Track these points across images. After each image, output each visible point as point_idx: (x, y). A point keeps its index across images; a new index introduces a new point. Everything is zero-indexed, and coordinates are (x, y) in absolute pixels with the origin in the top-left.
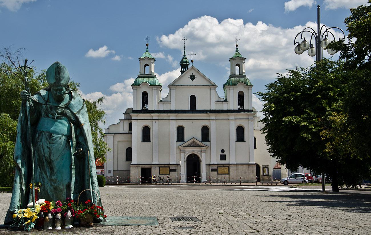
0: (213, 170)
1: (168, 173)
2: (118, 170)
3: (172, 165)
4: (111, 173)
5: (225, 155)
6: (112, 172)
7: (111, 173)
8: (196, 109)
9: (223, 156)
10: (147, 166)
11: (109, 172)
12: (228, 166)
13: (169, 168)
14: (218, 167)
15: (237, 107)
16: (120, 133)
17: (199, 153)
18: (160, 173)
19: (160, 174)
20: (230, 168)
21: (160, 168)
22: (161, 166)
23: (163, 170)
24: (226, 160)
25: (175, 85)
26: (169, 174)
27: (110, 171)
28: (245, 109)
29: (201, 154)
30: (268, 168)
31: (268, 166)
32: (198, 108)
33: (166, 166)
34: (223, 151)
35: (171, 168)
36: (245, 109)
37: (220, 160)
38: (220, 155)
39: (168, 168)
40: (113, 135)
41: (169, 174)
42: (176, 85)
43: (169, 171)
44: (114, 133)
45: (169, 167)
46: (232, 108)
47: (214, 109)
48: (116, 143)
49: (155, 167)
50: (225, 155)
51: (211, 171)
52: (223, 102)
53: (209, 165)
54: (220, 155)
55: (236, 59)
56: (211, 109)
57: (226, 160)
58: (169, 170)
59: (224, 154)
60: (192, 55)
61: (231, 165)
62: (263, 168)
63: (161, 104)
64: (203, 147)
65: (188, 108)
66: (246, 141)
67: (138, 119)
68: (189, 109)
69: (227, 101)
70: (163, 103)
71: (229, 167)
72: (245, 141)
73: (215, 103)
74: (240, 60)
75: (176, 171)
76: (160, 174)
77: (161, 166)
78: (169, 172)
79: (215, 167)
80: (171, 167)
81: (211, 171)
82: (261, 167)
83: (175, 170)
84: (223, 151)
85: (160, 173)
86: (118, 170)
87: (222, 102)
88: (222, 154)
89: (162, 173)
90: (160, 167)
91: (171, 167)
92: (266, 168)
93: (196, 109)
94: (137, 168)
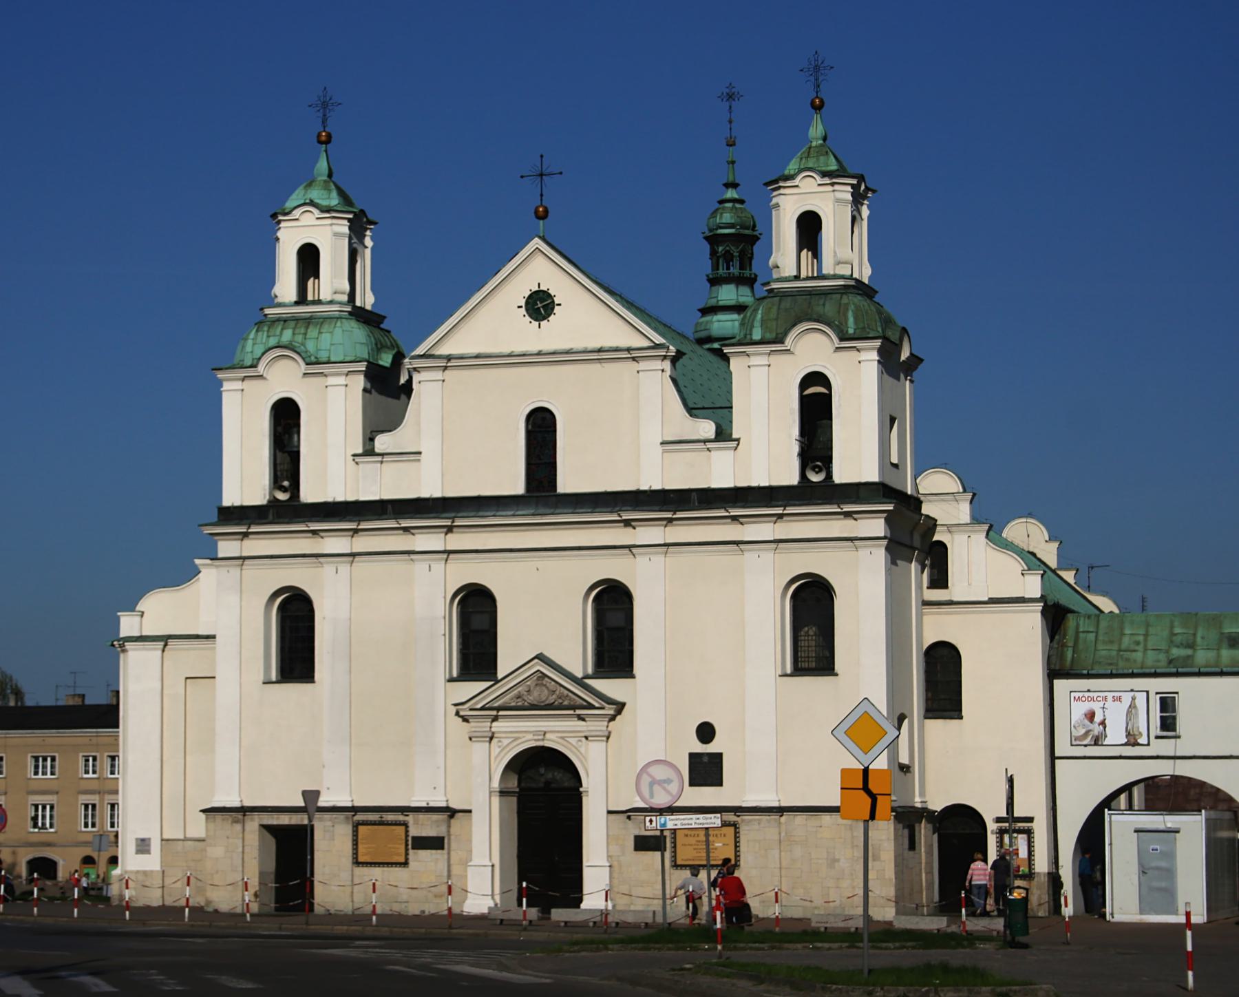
0: (644, 844)
1: (402, 860)
2: (186, 839)
3: (421, 816)
4: (148, 852)
5: (720, 755)
6: (156, 846)
7: (148, 852)
8: (561, 489)
9: (705, 759)
10: (290, 818)
11: (137, 845)
13: (407, 831)
15: (789, 476)
16: (197, 637)
17: (573, 741)
18: (361, 859)
19: (357, 862)
20: (743, 830)
21: (361, 828)
22: (360, 817)
23: (374, 841)
24: (721, 785)
25: (440, 357)
26: (405, 864)
27: (143, 840)
28: (838, 478)
30: (1029, 832)
31: (1031, 820)
32: (568, 481)
33: (390, 817)
34: (706, 732)
35: (414, 832)
36: (838, 478)
38: (692, 756)
39: (403, 828)
40: (161, 644)
41: (405, 864)
42: (449, 358)
43: (407, 845)
44: (165, 639)
45: (405, 825)
46: (760, 479)
47: (657, 486)
48: (175, 686)
49: (329, 823)
50: (720, 755)
52: (709, 445)
54: (692, 756)
55: (797, 182)
56: (644, 487)
57: (721, 785)
58: (407, 841)
59: (711, 748)
60: (541, 175)
61: (747, 817)
62: (1001, 832)
63: (369, 466)
64: (593, 707)
65: (517, 487)
67: (245, 554)
68: (519, 488)
69: (734, 436)
70: (379, 458)
72: (837, 675)
73: (664, 451)
74: (819, 185)
75: (442, 848)
76: (357, 862)
77: (360, 817)
78: (407, 854)
80: (416, 822)
82: (991, 826)
83: (436, 843)
84: (706, 732)
85: (361, 859)
86: (188, 835)
87: (705, 441)
88: (700, 748)
90: (356, 826)
91: (416, 822)
92: (1020, 831)
93: (561, 489)
94: (238, 827)
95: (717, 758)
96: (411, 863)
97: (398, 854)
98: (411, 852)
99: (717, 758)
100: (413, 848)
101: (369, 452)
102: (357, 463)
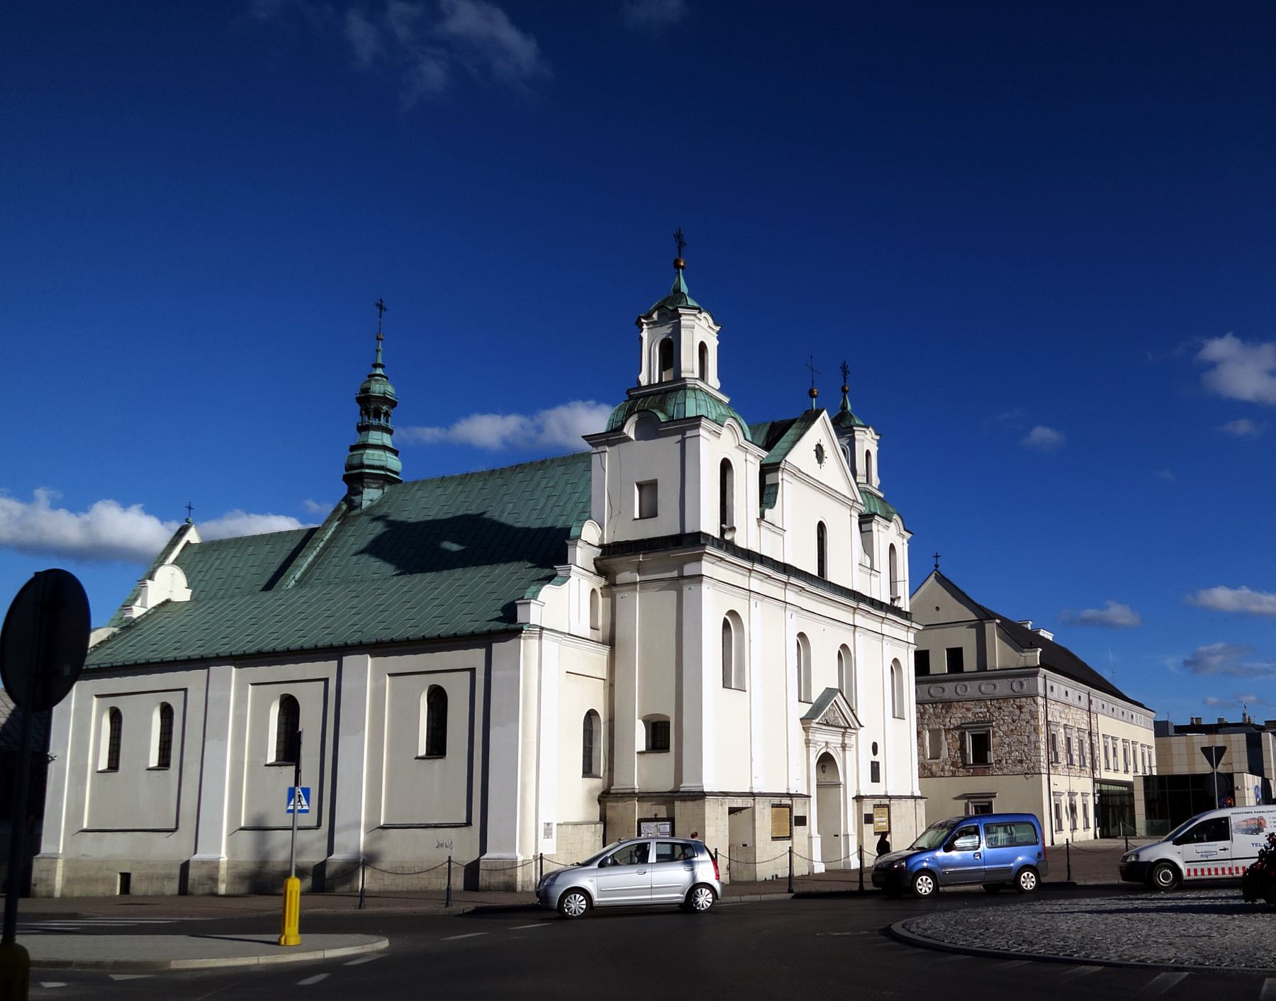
0: (869, 819)
12: (885, 803)
13: (791, 812)
14: (875, 806)
17: (838, 749)
20: (892, 808)
26: (790, 837)
29: (841, 755)
37: (872, 781)
43: (791, 823)
45: (790, 807)
51: (865, 823)
53: (859, 798)
58: (790, 819)
59: (876, 759)
66: (906, 717)
71: (888, 807)
78: (791, 830)
79: (868, 808)
81: (865, 823)
89: (789, 832)
95: (878, 763)
96: (795, 837)
97: (787, 830)
98: (794, 827)
99: (878, 763)
100: (795, 825)
101: (762, 516)
102: (759, 526)
